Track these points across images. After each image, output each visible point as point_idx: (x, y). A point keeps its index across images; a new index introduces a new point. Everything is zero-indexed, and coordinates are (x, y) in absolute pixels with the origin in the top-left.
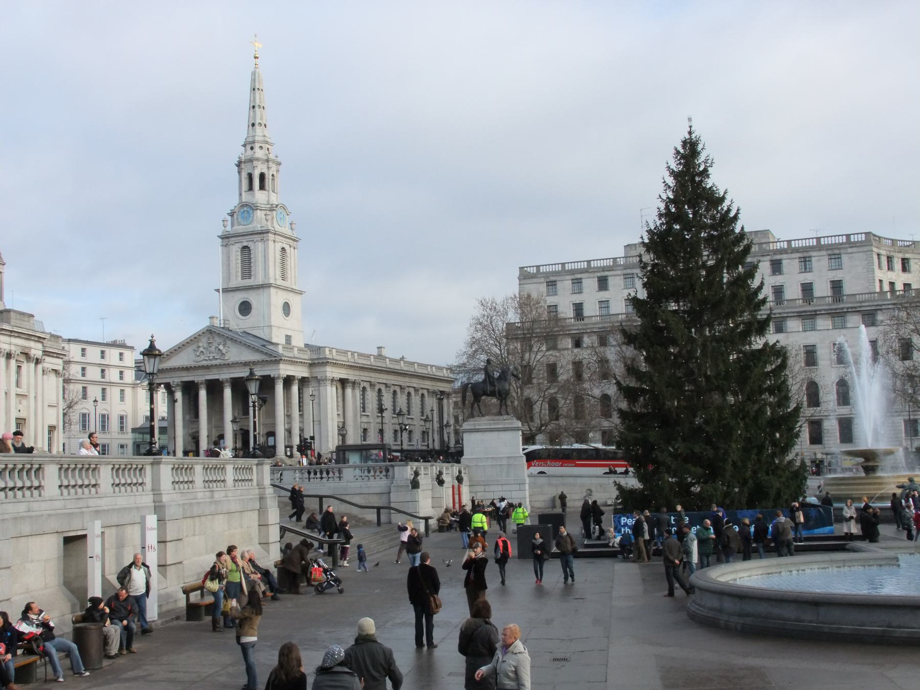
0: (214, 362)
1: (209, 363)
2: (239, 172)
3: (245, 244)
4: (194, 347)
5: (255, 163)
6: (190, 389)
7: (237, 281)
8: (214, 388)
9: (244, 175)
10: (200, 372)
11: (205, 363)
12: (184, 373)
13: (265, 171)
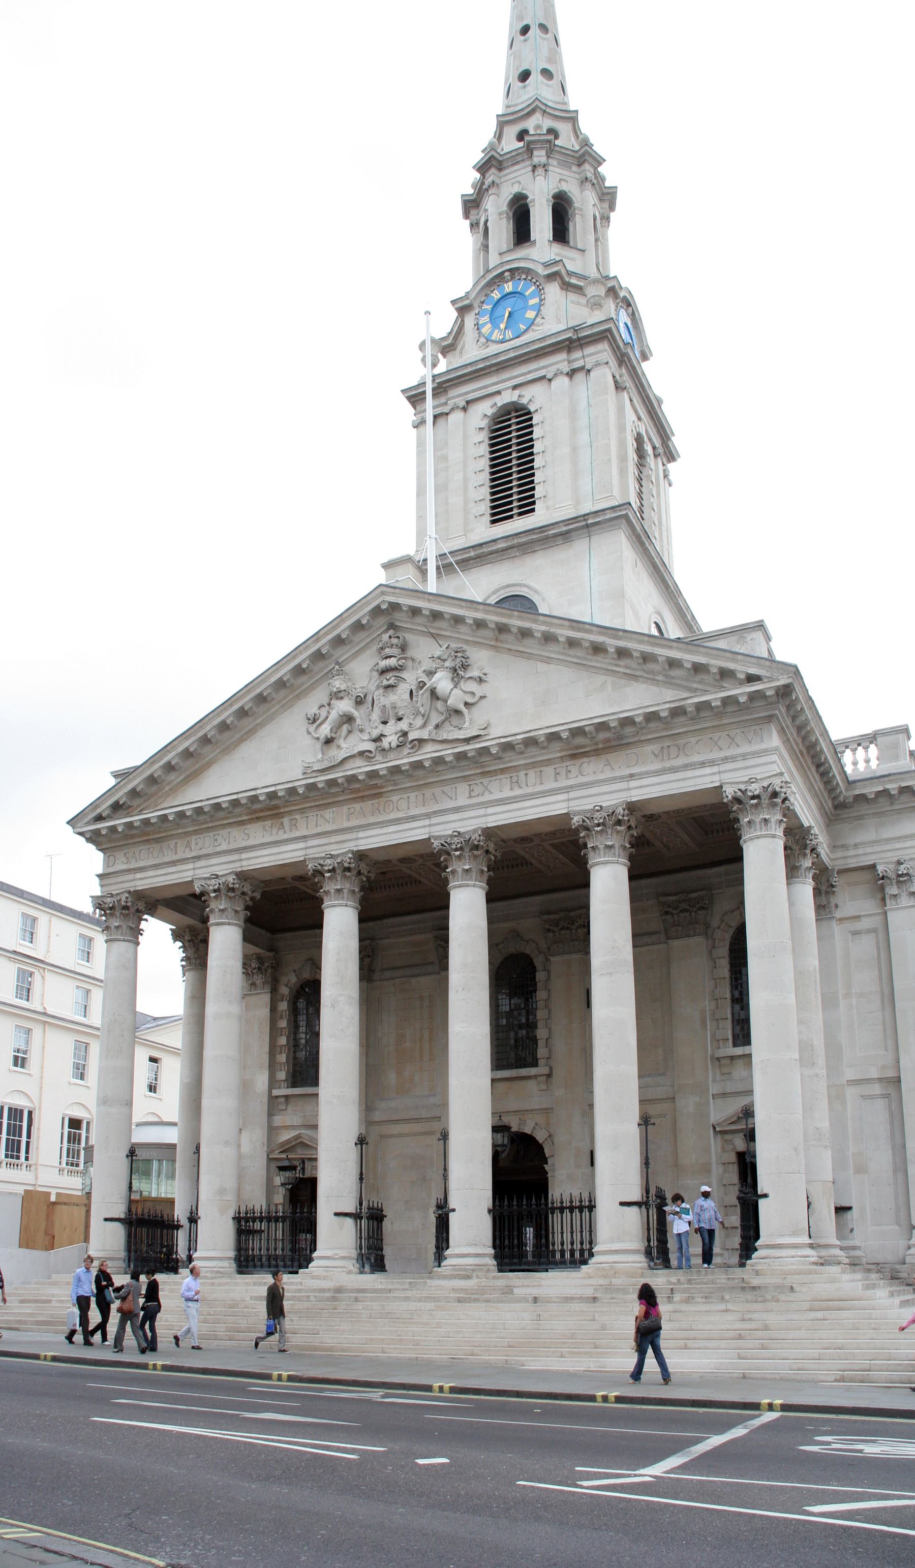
0: (404, 760)
1: (381, 765)
2: (474, 226)
3: (508, 397)
4: (311, 704)
5: (540, 156)
6: (280, 915)
7: (484, 531)
8: (403, 896)
9: (496, 208)
10: (332, 819)
11: (360, 768)
12: (257, 833)
13: (571, 188)
